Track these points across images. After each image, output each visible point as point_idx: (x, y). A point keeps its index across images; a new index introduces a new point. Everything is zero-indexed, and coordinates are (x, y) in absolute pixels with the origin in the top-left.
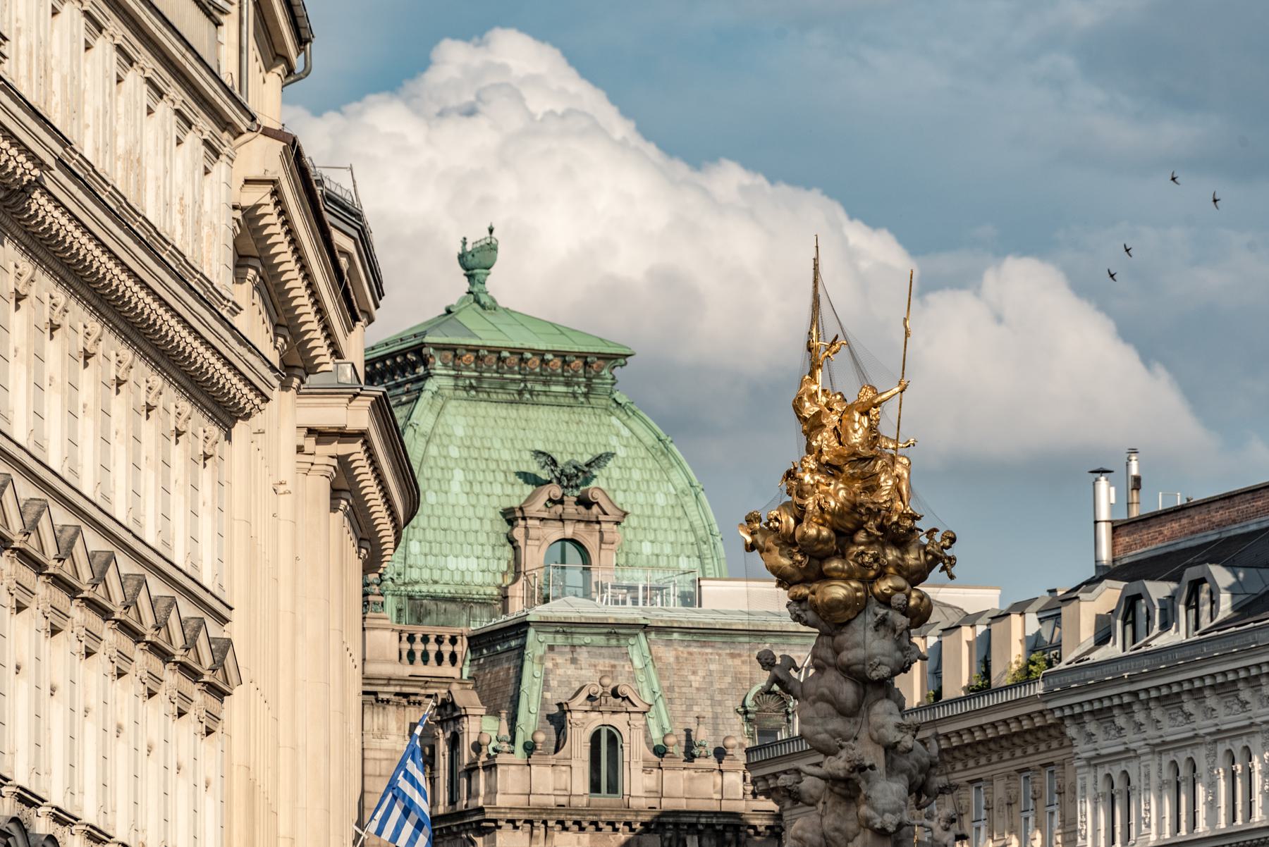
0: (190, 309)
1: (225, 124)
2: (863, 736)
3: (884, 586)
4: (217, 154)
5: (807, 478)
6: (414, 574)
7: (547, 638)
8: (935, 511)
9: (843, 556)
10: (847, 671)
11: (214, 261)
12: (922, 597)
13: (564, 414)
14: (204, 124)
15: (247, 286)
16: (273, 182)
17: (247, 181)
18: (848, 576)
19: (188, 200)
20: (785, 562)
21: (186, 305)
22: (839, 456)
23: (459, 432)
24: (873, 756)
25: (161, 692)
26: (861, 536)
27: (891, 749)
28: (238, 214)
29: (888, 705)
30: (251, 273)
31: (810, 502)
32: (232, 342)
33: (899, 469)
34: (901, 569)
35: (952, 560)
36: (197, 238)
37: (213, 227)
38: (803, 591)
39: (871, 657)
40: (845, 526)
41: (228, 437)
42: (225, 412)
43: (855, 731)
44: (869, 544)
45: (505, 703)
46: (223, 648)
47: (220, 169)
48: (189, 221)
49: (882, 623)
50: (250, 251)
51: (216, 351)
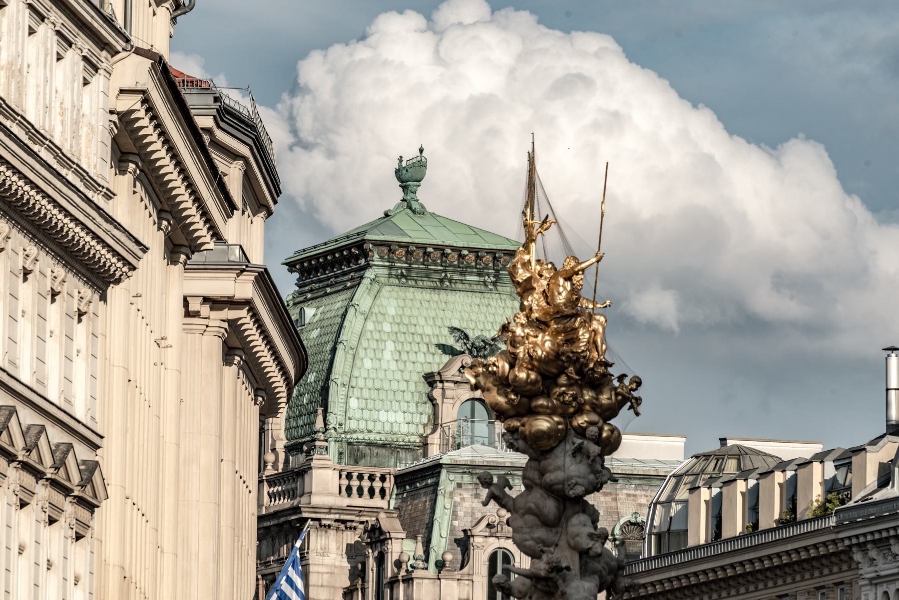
0: (60, 192)
1: (103, 44)
2: (563, 543)
3: (581, 420)
4: (96, 69)
5: (519, 331)
6: (353, 425)
7: (458, 478)
8: (624, 359)
9: (548, 395)
10: (550, 490)
11: (93, 153)
12: (613, 430)
13: (476, 299)
14: (84, 43)
15: (128, 178)
16: (143, 92)
17: (122, 91)
18: (552, 412)
19: (68, 105)
20: (501, 400)
21: (55, 188)
22: (546, 313)
23: (392, 311)
24: (568, 559)
25: (33, 503)
26: (563, 380)
27: (584, 554)
28: (115, 118)
29: (583, 518)
30: (132, 166)
31: (521, 351)
32: (99, 220)
33: (595, 325)
34: (596, 407)
35: (638, 400)
36: (75, 135)
37: (91, 126)
38: (516, 423)
39: (569, 478)
40: (549, 370)
41: (103, 298)
42: (100, 279)
43: (556, 539)
44: (569, 386)
45: (421, 528)
46: (90, 469)
47: (98, 81)
48: (68, 122)
49: (578, 451)
50: (126, 147)
51: (85, 227)
